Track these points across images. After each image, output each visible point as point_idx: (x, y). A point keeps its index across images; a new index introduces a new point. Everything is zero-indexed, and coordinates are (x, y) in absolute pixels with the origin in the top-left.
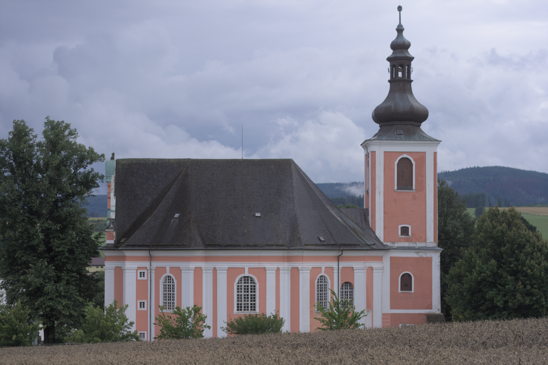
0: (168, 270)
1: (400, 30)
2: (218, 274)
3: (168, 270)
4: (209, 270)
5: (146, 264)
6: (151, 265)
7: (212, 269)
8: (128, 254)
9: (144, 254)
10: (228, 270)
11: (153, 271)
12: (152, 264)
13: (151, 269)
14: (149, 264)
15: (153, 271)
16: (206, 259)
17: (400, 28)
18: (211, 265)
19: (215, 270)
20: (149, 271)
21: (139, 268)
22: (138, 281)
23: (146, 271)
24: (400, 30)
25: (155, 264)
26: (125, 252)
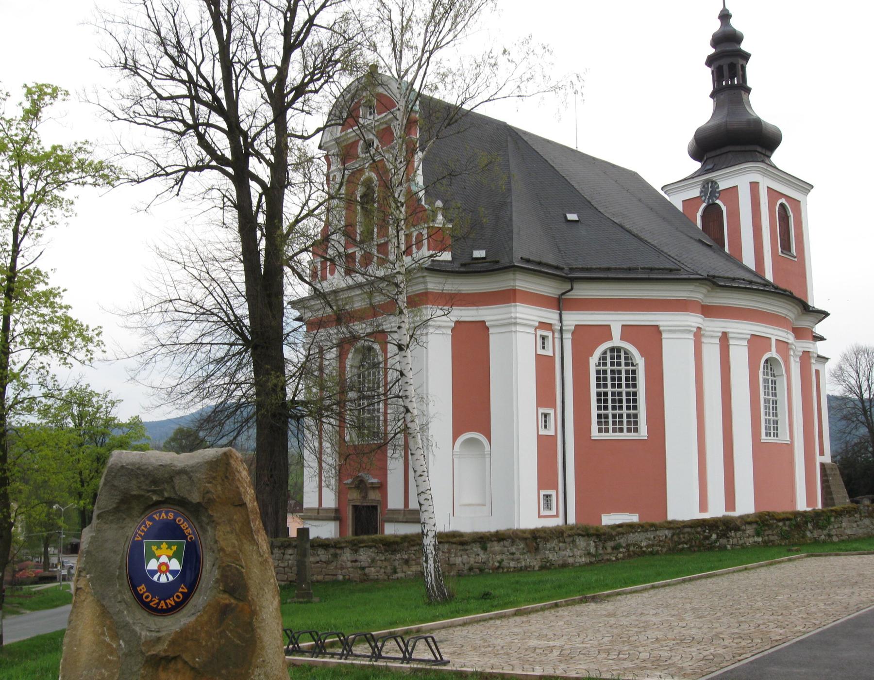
0: (616, 332)
1: (725, 16)
2: (731, 348)
3: (616, 332)
4: (712, 337)
5: (551, 316)
6: (561, 321)
7: (720, 334)
8: (523, 283)
9: (548, 288)
10: (749, 341)
11: (568, 336)
12: (564, 317)
13: (561, 331)
14: (557, 317)
15: (568, 336)
16: (708, 311)
17: (725, 13)
18: (715, 326)
19: (724, 338)
20: (557, 335)
21: (543, 325)
22: (538, 357)
23: (549, 334)
24: (725, 16)
25: (572, 319)
26: (519, 276)
